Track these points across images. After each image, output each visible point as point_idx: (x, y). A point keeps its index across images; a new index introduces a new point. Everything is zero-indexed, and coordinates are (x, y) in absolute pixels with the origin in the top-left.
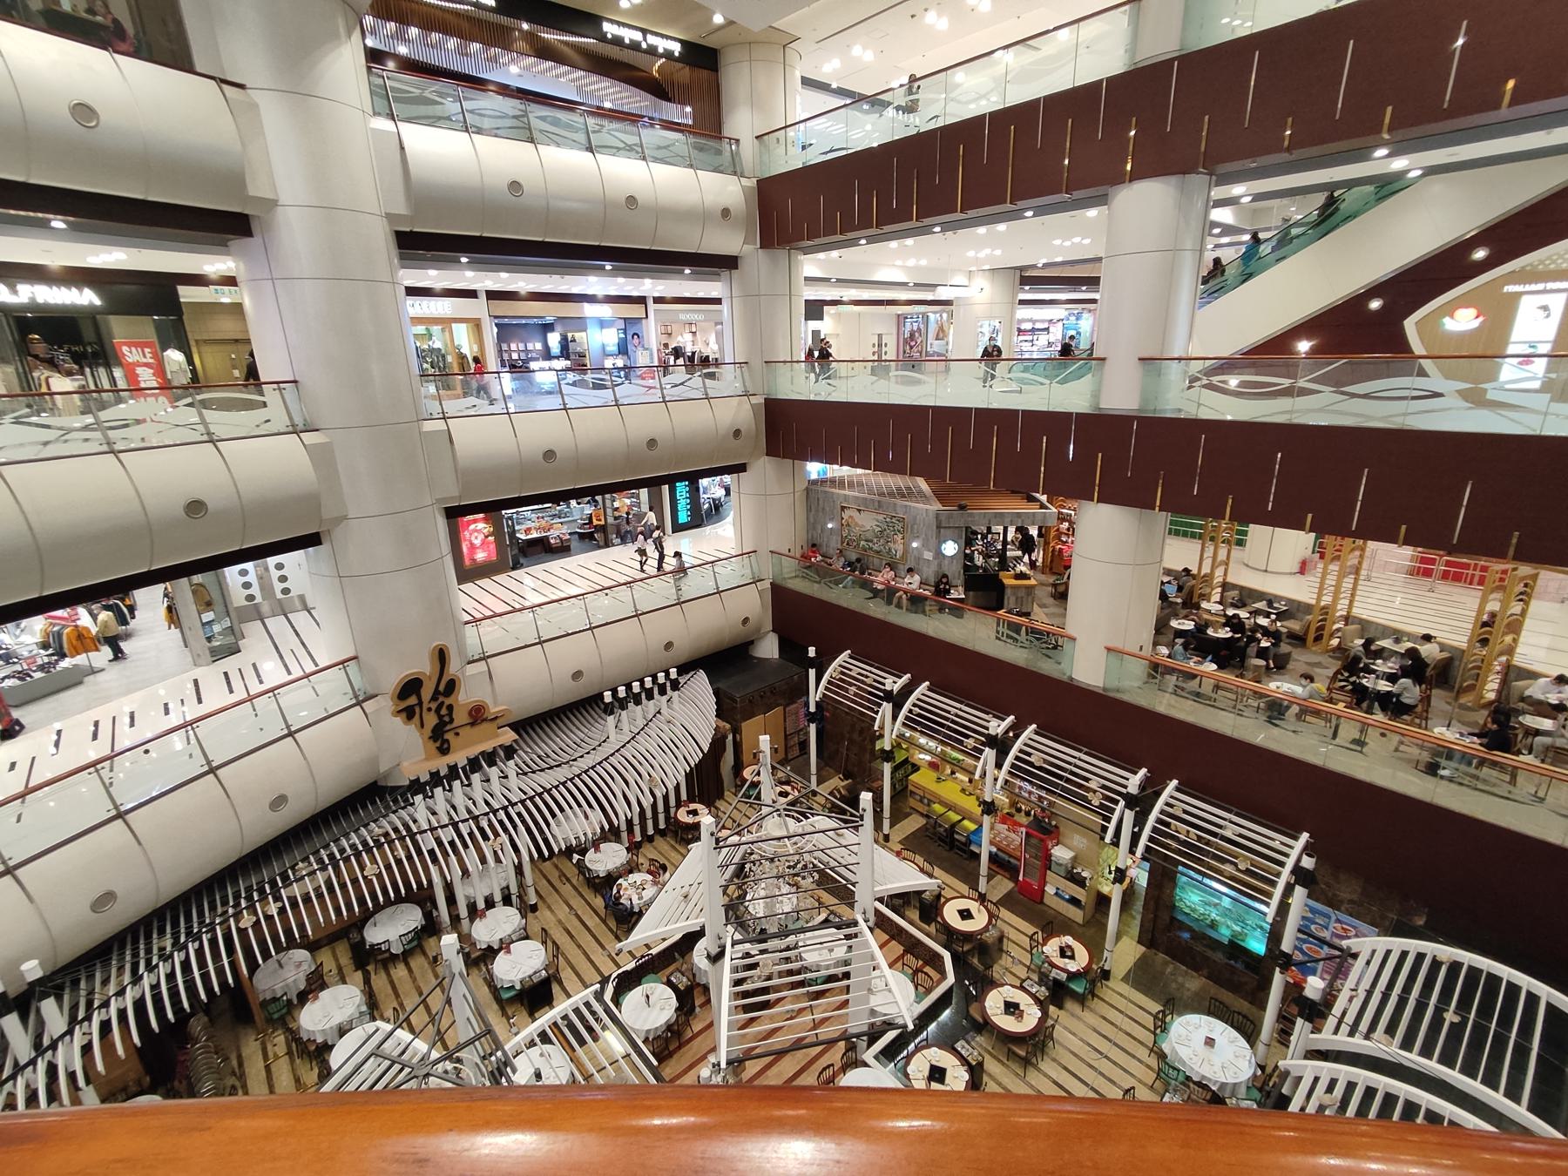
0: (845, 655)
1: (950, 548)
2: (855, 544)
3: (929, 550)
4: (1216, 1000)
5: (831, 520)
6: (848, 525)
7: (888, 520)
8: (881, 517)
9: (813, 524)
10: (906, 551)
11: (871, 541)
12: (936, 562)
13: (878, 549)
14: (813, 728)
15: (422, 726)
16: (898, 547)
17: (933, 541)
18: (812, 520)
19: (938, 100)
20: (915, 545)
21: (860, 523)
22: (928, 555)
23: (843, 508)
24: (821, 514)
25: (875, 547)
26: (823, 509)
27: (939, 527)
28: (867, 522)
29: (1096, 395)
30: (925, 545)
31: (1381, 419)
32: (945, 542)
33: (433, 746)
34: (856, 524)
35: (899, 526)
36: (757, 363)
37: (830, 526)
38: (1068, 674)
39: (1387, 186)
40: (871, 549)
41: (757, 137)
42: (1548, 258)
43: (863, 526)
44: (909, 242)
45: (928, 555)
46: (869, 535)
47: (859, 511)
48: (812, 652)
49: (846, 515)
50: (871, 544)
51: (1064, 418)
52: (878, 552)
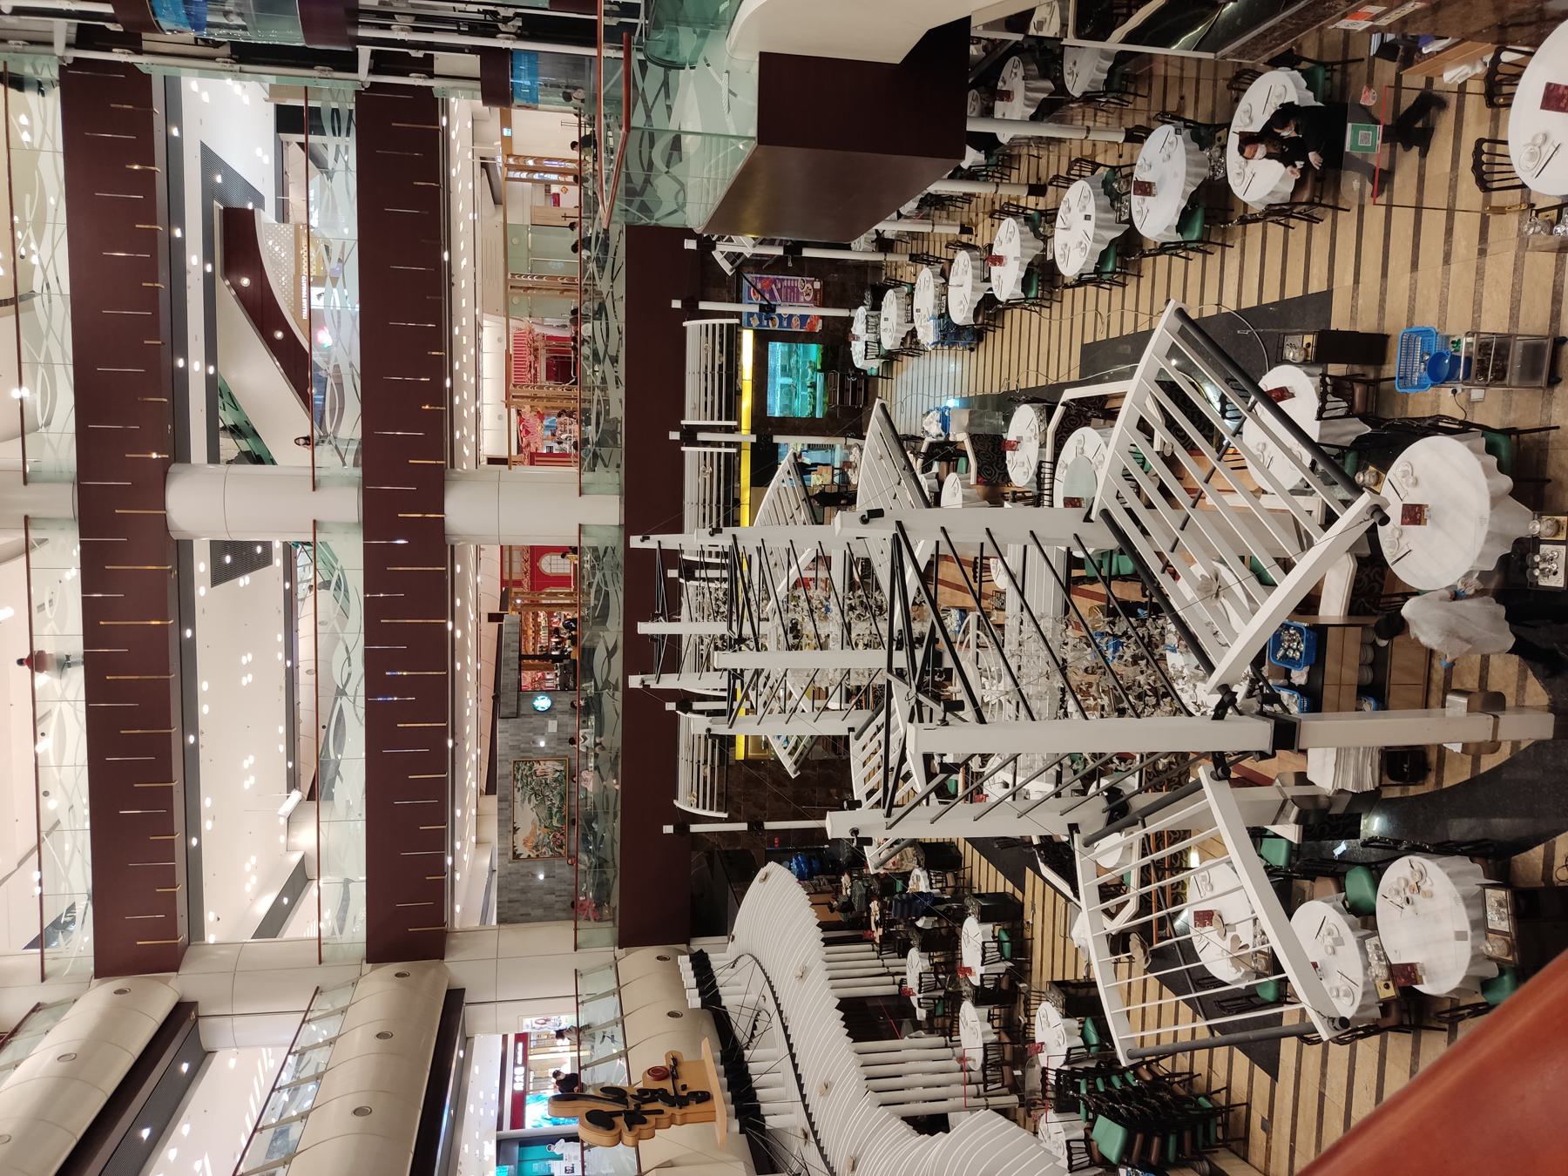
0: (677, 804)
1: (542, 703)
2: (558, 835)
3: (546, 725)
4: (866, 355)
5: (534, 876)
6: (536, 847)
7: (519, 785)
8: (518, 796)
9: (548, 914)
10: (555, 758)
11: (550, 809)
12: (559, 716)
13: (558, 798)
15: (661, 1112)
16: (550, 768)
17: (536, 721)
18: (539, 912)
19: (60, 710)
20: (542, 744)
21: (530, 828)
22: (552, 726)
23: (516, 856)
24: (530, 895)
25: (557, 803)
26: (523, 891)
27: (517, 715)
28: (527, 816)
29: (347, 527)
30: (541, 731)
31: (354, 321)
32: (535, 709)
33: (694, 1107)
34: (533, 833)
35: (525, 768)
36: (320, 976)
37: (541, 877)
38: (617, 530)
39: (216, 390)
40: (560, 808)
41: (43, 979)
42: (283, 293)
43: (533, 823)
44: (206, 802)
45: (552, 726)
46: (544, 814)
47: (515, 830)
48: (668, 829)
49: (524, 851)
50: (555, 810)
51: (368, 551)
52: (562, 799)
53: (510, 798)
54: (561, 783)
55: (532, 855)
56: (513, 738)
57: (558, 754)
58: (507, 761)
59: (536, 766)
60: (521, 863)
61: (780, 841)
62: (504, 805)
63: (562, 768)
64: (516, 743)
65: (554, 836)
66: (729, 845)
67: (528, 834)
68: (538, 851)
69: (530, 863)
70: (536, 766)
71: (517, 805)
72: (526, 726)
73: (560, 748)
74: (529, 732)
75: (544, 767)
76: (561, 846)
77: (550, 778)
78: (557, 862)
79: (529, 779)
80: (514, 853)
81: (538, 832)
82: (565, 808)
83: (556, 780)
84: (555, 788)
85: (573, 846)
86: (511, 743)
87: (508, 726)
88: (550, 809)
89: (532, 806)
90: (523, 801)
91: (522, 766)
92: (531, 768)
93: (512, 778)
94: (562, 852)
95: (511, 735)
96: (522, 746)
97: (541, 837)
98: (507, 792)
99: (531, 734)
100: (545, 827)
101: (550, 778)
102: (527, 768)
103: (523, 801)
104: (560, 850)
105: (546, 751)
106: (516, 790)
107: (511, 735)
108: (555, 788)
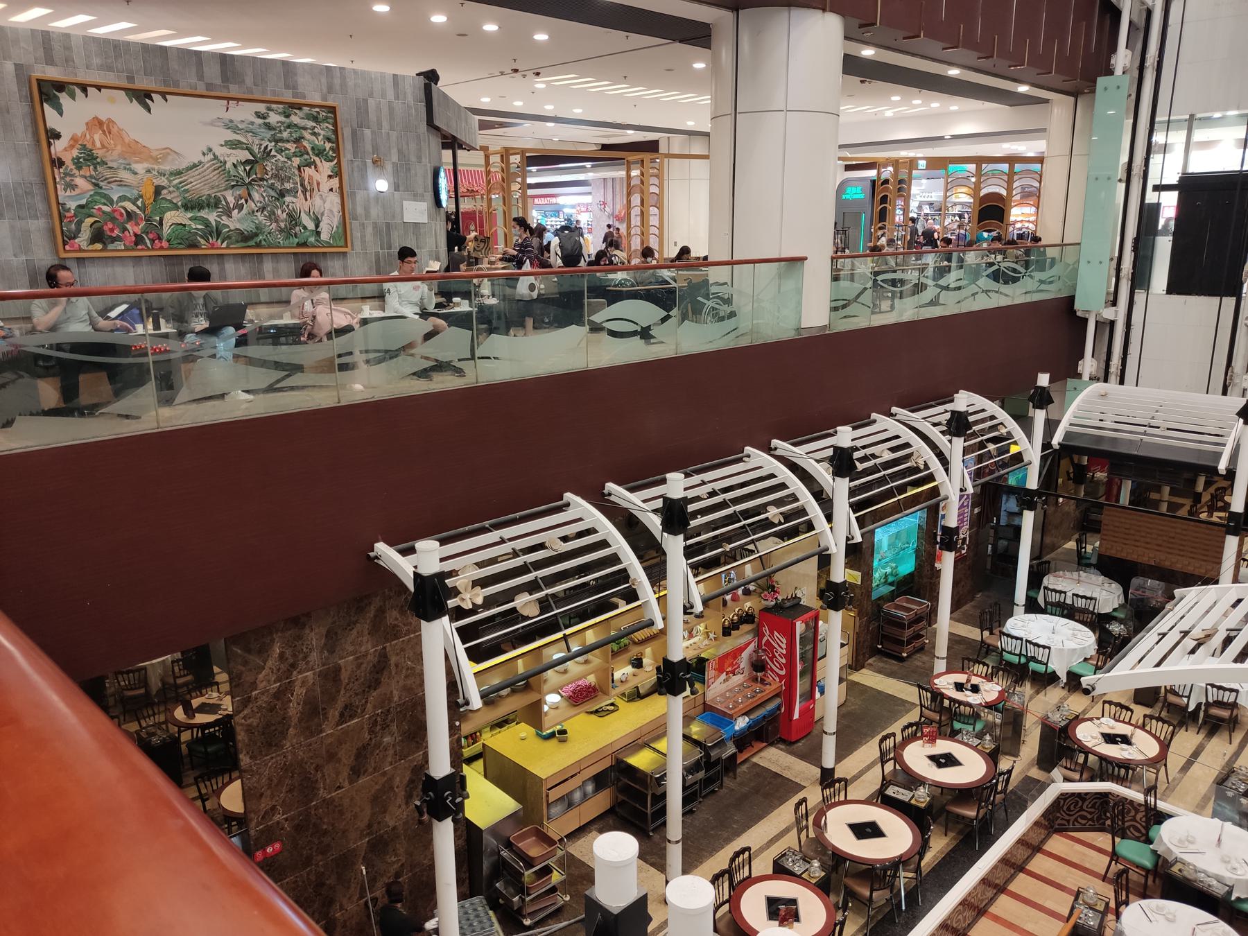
6: (88, 158)
7: (274, 118)
8: (244, 113)
11: (213, 203)
13: (247, 226)
14: (1028, 519)
21: (153, 142)
25: (236, 222)
34: (135, 150)
35: (317, 137)
43: (167, 152)
46: (200, 186)
47: (143, 97)
50: (212, 217)
52: (245, 237)
53: (234, 91)
54: (288, 232)
55: (59, 147)
56: (385, 110)
57: (356, 224)
58: (330, 89)
59: (326, 167)
60: (19, 110)
61: (276, 855)
62: (213, 73)
63: (325, 236)
64: (372, 116)
65: (130, 215)
66: (249, 730)
67: (134, 134)
68: (78, 164)
69: (24, 138)
70: (326, 167)
71: (216, 109)
72: (413, 146)
73: (369, 230)
74: (400, 152)
75: (325, 186)
76: (98, 236)
77: (297, 202)
78: (37, 226)
79: (292, 147)
80: (61, 86)
81: (140, 168)
82: (222, 247)
83: (294, 219)
84: (272, 217)
85: (97, 276)
86: (372, 103)
87: (410, 99)
88: (213, 203)
89: (221, 151)
90: (230, 125)
91: (324, 130)
92: (320, 152)
93: (288, 97)
94: (83, 240)
95: (391, 109)
96: (367, 132)
97: (125, 175)
98: (249, 80)
99: (395, 158)
100: (158, 190)
101: (297, 202)
102: (319, 142)
103: (230, 125)
104: (83, 240)
105: (360, 196)
106: (261, 108)
107: (391, 109)
108: (272, 217)
